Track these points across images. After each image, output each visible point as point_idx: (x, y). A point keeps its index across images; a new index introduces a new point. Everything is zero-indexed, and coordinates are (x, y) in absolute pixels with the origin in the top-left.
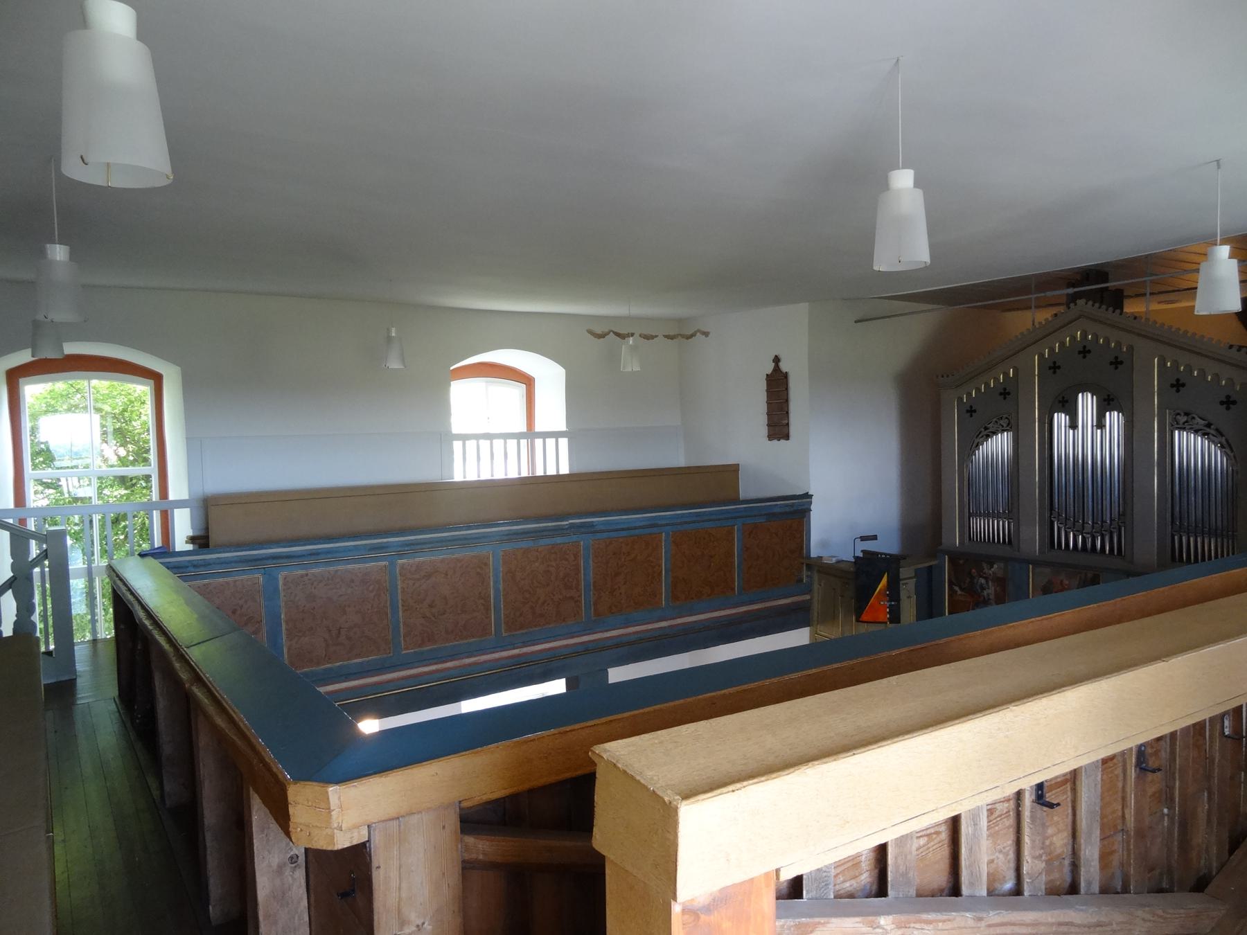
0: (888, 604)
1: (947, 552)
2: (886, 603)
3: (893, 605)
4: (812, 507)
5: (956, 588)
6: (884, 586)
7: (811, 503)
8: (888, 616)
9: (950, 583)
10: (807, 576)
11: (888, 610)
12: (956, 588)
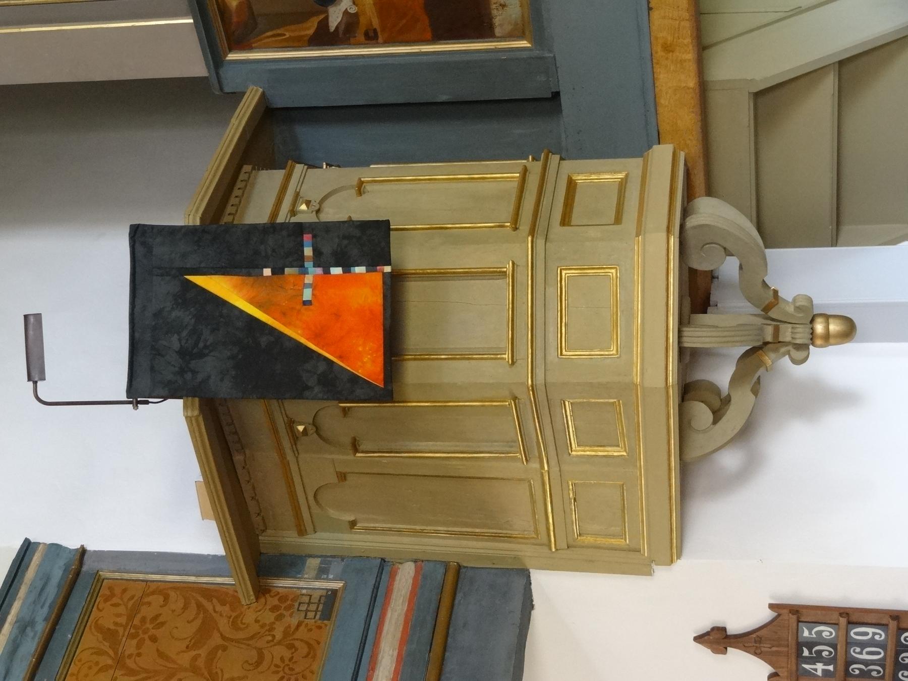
0: (313, 272)
1: (216, 59)
2: (308, 279)
3: (317, 253)
4: (72, 543)
5: (335, 17)
6: (238, 288)
7: (55, 549)
8: (360, 270)
9: (323, 37)
10: (322, 572)
11: (336, 271)
12: (335, 17)
